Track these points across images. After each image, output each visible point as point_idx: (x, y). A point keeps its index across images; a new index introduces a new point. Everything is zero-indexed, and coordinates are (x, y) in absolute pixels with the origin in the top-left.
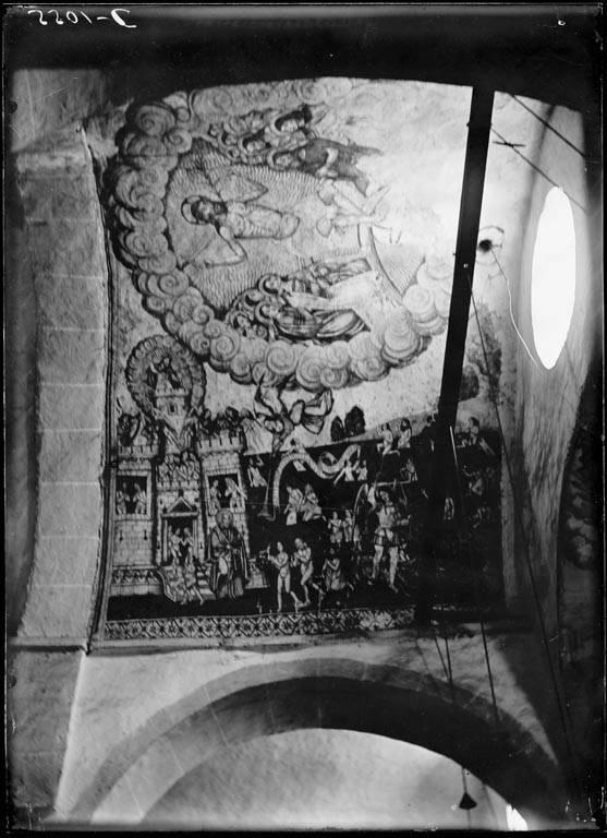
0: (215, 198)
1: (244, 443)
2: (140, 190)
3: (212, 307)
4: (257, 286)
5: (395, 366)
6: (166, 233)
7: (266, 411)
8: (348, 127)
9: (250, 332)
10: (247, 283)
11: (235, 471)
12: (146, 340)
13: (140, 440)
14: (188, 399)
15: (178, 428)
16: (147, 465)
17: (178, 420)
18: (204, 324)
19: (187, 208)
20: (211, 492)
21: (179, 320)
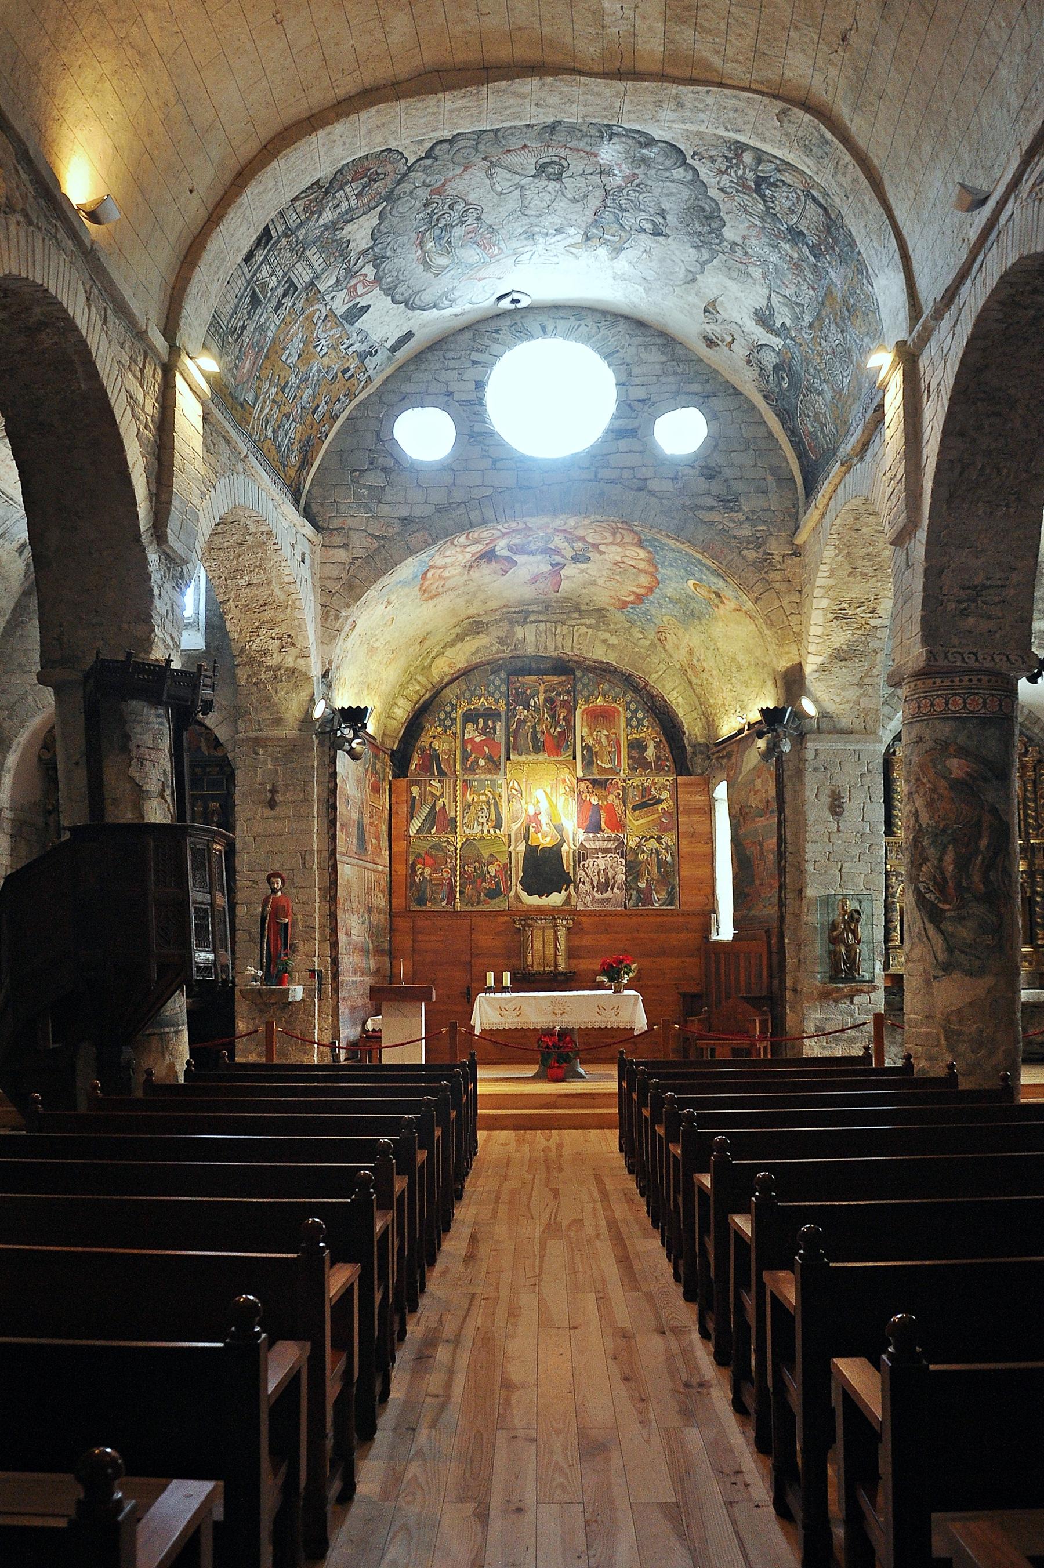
0: (564, 175)
1: (324, 271)
2: (579, 135)
3: (443, 185)
4: (467, 204)
5: (406, 305)
6: (525, 146)
7: (352, 263)
8: (642, 249)
9: (422, 215)
10: (472, 197)
11: (299, 286)
12: (401, 153)
13: (300, 205)
14: (349, 210)
15: (321, 222)
16: (280, 230)
17: (328, 216)
18: (425, 184)
19: (554, 158)
20: (280, 291)
21: (425, 169)
